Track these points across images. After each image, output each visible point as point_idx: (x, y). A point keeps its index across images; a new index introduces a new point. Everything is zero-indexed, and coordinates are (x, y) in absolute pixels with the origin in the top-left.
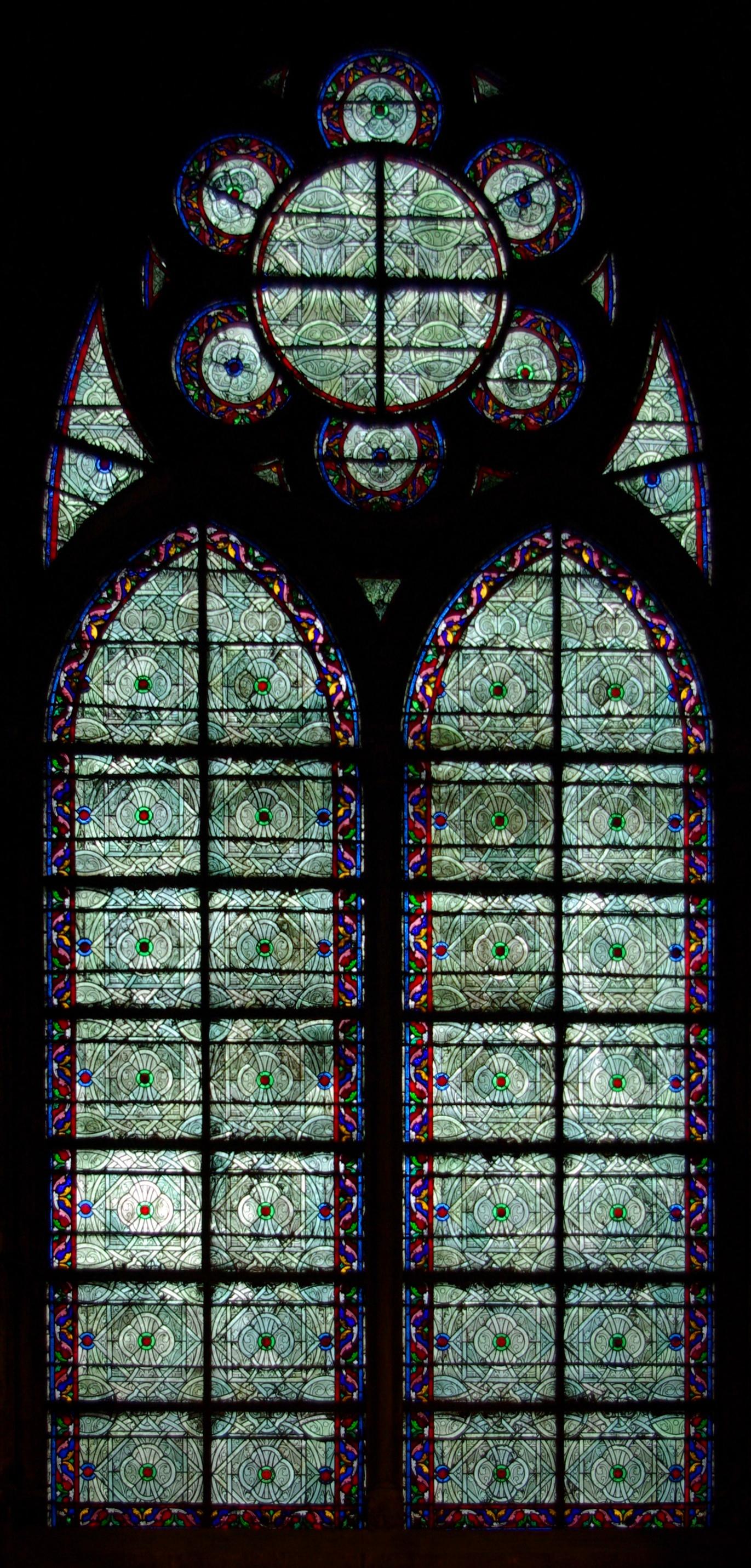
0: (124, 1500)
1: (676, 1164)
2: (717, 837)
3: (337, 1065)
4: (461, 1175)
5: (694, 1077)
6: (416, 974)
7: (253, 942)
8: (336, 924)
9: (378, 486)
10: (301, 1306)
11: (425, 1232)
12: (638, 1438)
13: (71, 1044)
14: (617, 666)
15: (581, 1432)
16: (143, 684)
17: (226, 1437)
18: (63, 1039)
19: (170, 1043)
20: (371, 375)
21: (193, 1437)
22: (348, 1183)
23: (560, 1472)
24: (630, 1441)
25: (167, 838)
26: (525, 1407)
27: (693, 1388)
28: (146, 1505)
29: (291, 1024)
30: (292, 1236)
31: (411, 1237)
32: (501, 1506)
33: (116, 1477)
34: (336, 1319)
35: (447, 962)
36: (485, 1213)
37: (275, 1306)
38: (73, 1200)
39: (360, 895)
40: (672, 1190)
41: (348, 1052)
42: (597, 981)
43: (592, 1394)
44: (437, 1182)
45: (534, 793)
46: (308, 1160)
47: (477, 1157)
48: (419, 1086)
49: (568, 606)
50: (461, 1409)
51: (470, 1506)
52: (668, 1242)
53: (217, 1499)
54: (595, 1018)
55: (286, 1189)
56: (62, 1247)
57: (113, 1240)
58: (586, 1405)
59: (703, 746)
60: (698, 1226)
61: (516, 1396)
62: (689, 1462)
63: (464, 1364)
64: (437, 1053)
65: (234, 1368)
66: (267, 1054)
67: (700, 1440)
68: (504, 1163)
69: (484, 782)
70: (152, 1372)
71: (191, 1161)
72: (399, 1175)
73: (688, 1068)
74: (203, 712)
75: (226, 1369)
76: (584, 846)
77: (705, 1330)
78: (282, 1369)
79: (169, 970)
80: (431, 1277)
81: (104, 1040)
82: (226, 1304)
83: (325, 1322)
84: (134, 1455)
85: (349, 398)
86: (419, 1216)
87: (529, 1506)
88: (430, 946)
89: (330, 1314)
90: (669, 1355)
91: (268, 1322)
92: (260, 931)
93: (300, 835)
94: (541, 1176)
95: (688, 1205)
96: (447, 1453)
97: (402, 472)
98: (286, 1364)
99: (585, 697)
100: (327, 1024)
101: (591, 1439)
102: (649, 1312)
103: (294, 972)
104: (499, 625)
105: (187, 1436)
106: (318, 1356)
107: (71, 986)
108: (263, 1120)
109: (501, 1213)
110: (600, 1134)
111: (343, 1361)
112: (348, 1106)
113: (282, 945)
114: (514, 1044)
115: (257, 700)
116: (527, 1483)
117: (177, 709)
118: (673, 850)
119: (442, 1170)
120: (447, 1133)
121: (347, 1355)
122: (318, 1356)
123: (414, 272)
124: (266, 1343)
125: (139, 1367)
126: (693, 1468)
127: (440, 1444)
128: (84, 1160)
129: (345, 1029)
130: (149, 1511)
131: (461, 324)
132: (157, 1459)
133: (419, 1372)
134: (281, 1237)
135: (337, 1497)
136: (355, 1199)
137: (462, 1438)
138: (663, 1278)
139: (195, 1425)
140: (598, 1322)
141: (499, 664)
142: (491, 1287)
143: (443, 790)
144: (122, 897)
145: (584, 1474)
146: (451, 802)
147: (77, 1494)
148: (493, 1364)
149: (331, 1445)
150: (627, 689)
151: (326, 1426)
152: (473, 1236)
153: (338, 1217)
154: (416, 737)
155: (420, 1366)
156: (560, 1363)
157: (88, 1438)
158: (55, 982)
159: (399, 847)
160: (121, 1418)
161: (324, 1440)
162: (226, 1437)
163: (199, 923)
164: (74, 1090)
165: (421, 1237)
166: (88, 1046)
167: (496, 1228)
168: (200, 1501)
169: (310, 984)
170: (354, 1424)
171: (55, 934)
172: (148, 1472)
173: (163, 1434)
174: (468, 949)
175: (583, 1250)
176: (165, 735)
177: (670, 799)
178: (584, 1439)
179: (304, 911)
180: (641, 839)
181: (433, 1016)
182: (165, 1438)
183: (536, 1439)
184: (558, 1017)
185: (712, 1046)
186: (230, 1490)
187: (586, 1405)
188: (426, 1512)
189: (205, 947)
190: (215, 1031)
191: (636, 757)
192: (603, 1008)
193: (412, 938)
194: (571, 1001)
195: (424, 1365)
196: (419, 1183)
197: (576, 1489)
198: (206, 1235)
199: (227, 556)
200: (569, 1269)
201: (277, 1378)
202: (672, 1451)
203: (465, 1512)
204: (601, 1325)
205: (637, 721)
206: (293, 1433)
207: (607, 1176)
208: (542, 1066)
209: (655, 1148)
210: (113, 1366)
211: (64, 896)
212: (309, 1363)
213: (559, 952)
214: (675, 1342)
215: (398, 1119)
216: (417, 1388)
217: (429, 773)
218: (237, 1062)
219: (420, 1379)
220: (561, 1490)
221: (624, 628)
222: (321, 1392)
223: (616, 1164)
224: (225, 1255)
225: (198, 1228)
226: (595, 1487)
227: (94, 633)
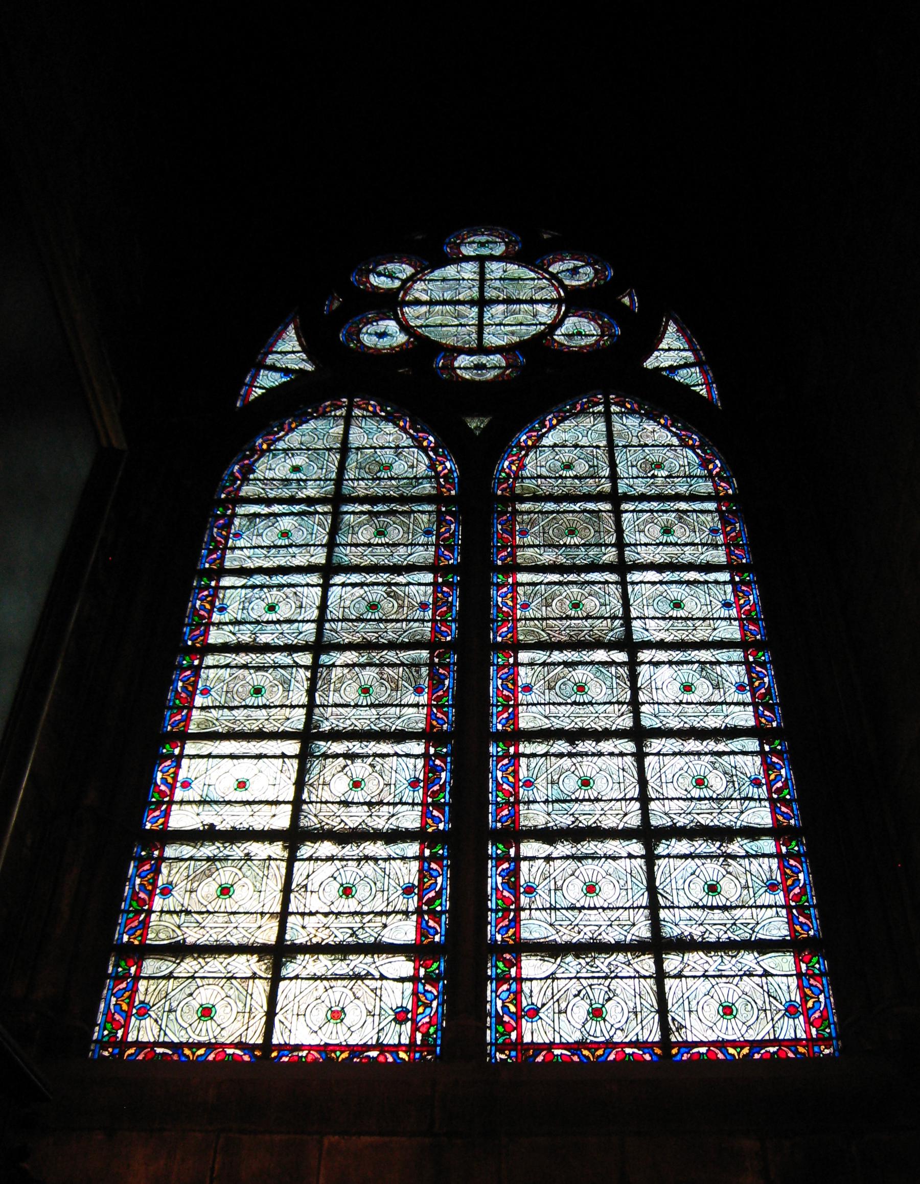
0: (176, 1040)
1: (752, 744)
2: (751, 537)
5: (757, 684)
6: (503, 620)
7: (364, 603)
8: (435, 592)
9: (477, 378)
10: (385, 860)
11: (512, 799)
12: (745, 975)
13: (197, 670)
14: (656, 455)
15: (682, 970)
16: (296, 469)
18: (191, 667)
20: (474, 336)
21: (261, 978)
22: (438, 762)
23: (663, 1009)
24: (737, 978)
25: (302, 546)
26: (618, 947)
27: (798, 928)
28: (199, 1045)
29: (392, 653)
30: (381, 803)
31: (497, 803)
32: (598, 1045)
33: (172, 1016)
34: (421, 871)
36: (570, 785)
37: (359, 860)
38: (175, 779)
40: (750, 764)
41: (441, 671)
42: (661, 623)
43: (690, 934)
44: (523, 761)
45: (599, 518)
46: (400, 746)
47: (560, 742)
48: (505, 692)
49: (617, 427)
51: (562, 1045)
52: (752, 804)
55: (377, 768)
56: (157, 813)
57: (207, 807)
58: (684, 945)
59: (730, 492)
60: (778, 791)
62: (804, 998)
63: (553, 908)
64: (522, 671)
65: (311, 914)
66: (370, 674)
67: (814, 976)
69: (558, 512)
71: (292, 747)
72: (488, 755)
73: (750, 679)
74: (339, 480)
75: (303, 914)
76: (641, 545)
77: (801, 876)
78: (362, 914)
79: (289, 621)
80: (515, 834)
81: (227, 666)
82: (310, 859)
83: (410, 873)
85: (459, 344)
86: (505, 786)
87: (631, 1044)
88: (515, 604)
89: (415, 865)
90: (768, 898)
91: (350, 873)
94: (622, 754)
95: (767, 776)
96: (534, 993)
97: (496, 372)
98: (365, 910)
99: (634, 469)
100: (425, 654)
101: (694, 977)
102: (742, 861)
103: (397, 621)
104: (566, 436)
105: (254, 977)
107: (206, 633)
110: (674, 724)
111: (425, 908)
112: (440, 707)
113: (389, 607)
115: (382, 474)
116: (627, 1019)
117: (320, 480)
119: (528, 752)
120: (531, 725)
121: (431, 901)
123: (502, 296)
124: (347, 891)
126: (810, 1004)
127: (528, 983)
128: (191, 748)
131: (535, 316)
134: (370, 804)
136: (443, 775)
137: (552, 977)
138: (752, 833)
139: (264, 967)
140: (690, 871)
141: (567, 455)
142: (579, 843)
143: (525, 517)
144: (258, 579)
145: (690, 1012)
146: (533, 523)
147: (126, 1034)
148: (583, 908)
149: (409, 986)
151: (403, 966)
152: (558, 801)
153: (426, 789)
154: (503, 490)
155: (506, 911)
157: (149, 978)
158: (192, 631)
159: (490, 547)
160: (187, 961)
161: (402, 980)
163: (320, 593)
164: (193, 700)
165: (508, 803)
166: (212, 671)
167: (581, 794)
168: (260, 1041)
169: (411, 628)
170: (435, 965)
171: (198, 603)
172: (207, 1012)
174: (548, 605)
176: (311, 491)
177: (709, 518)
178: (686, 977)
179: (409, 584)
180: (688, 541)
181: (517, 646)
182: (232, 978)
183: (634, 977)
184: (629, 645)
185: (769, 662)
187: (684, 945)
188: (513, 1053)
189: (323, 607)
190: (324, 659)
191: (678, 497)
192: (668, 639)
193: (500, 599)
194: (637, 636)
195: (511, 910)
196: (506, 761)
198: (297, 804)
199: (368, 411)
200: (656, 827)
201: (355, 922)
202: (784, 988)
203: (557, 1052)
204: (693, 874)
205: (676, 480)
206: (368, 973)
208: (617, 678)
209: (732, 733)
210: (188, 913)
211: (211, 580)
212: (390, 909)
214: (772, 887)
215: (489, 716)
217: (514, 508)
218: (341, 680)
219: (506, 922)
223: (693, 745)
226: (701, 1025)
227: (265, 446)
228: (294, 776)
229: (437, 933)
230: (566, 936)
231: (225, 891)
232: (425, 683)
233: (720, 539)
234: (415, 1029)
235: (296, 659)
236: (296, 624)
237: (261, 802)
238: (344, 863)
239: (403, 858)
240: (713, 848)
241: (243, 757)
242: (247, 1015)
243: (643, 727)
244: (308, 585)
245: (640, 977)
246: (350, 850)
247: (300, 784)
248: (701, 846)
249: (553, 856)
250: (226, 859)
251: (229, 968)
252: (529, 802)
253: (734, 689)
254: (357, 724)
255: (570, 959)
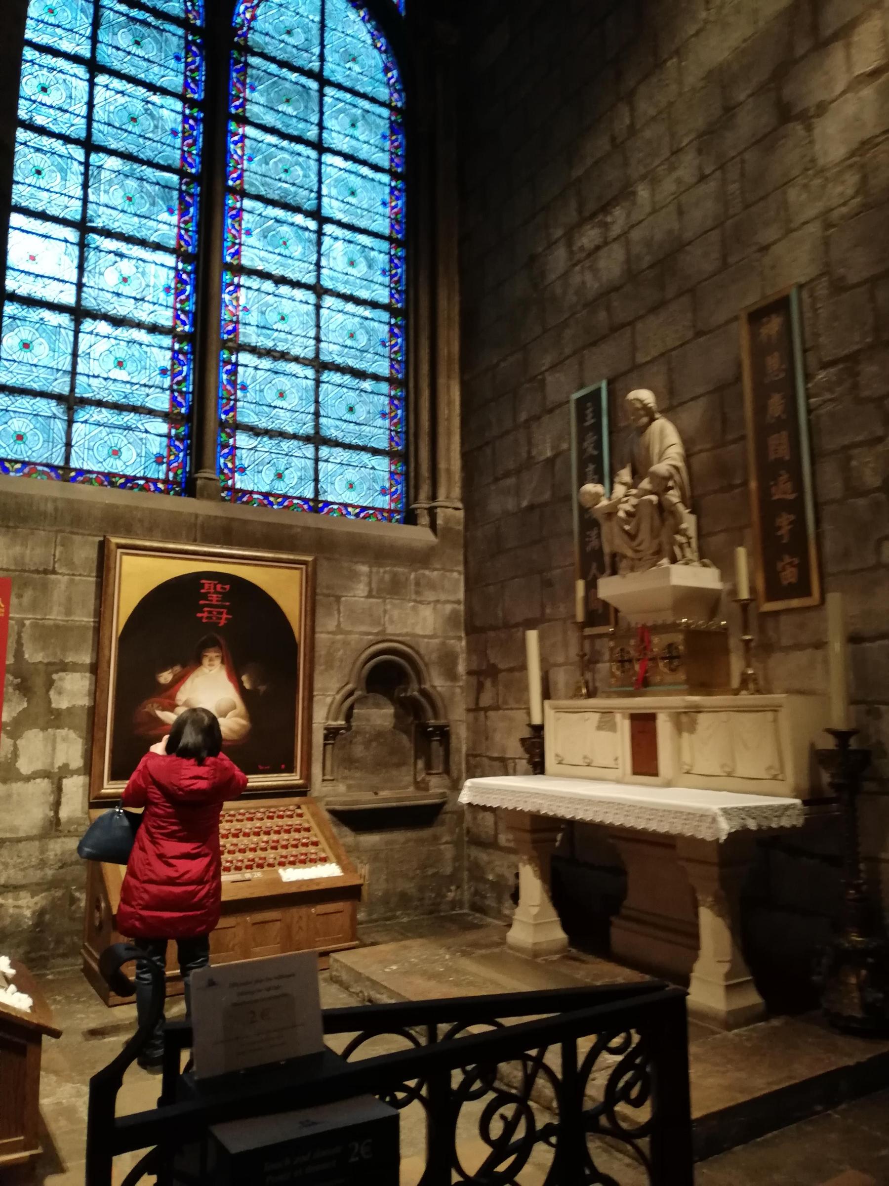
3: (180, 204)
4: (258, 290)
7: (126, 114)
10: (148, 346)
17: (86, 422)
19: (60, 156)
21: (59, 418)
23: (316, 480)
26: (295, 437)
28: (16, 461)
30: (142, 299)
32: (279, 496)
35: (253, 166)
37: (129, 342)
39: (200, 111)
42: (342, 205)
50: (255, 431)
53: (75, 463)
54: (339, 224)
55: (140, 270)
61: (290, 430)
64: (245, 216)
65: (94, 376)
66: (132, 184)
68: (284, 290)
70: (29, 368)
82: (91, 333)
83: (164, 359)
84: (9, 423)
88: (243, 155)
89: (169, 354)
90: (380, 422)
92: (131, 109)
93: (162, 62)
94: (307, 303)
96: (244, 457)
98: (134, 381)
100: (175, 178)
106: (158, 380)
108: (126, 224)
109: (283, 318)
112: (187, 230)
113: (146, 122)
114: (292, 224)
116: (295, 483)
118: (383, 150)
121: (179, 383)
122: (158, 380)
124: (120, 364)
125: (19, 362)
129: (187, 184)
130: (18, 466)
132: (28, 429)
133: (228, 404)
135: (167, 474)
137: (254, 449)
138: (376, 377)
139: (61, 410)
146: (259, 79)
148: (275, 407)
150: (359, 59)
151: (162, 427)
155: (229, 400)
156: (317, 414)
162: (86, 422)
169: (164, 151)
172: (20, 437)
173: (35, 413)
174: (267, 164)
175: (331, 352)
179: (162, 107)
182: (36, 415)
186: (86, 459)
189: (90, 105)
191: (364, 96)
197: (325, 492)
201: (127, 388)
203: (255, 496)
206: (137, 427)
207: (346, 313)
209: (374, 305)
212: (151, 383)
213: (320, 182)
214: (384, 415)
216: (226, 413)
218: (110, 182)
220: (317, 492)
221: (358, 29)
222: (159, 404)
223: (350, 307)
224: (93, 301)
225: (75, 280)
226: (336, 492)
228: (76, 262)
229: (182, 406)
230: (263, 424)
231: (26, 346)
232: (175, 203)
233: (387, 145)
234: (169, 470)
235: (70, 150)
236: (68, 114)
237: (49, 278)
238: (117, 342)
239: (161, 347)
240: (355, 382)
241: (33, 233)
242: (51, 444)
243: (321, 286)
244: (75, 76)
245: (306, 458)
246: (123, 333)
247: (81, 269)
248: (347, 379)
249: (259, 367)
250: (24, 319)
251: (35, 407)
252: (245, 324)
253: (379, 272)
254: (123, 226)
255: (265, 439)
